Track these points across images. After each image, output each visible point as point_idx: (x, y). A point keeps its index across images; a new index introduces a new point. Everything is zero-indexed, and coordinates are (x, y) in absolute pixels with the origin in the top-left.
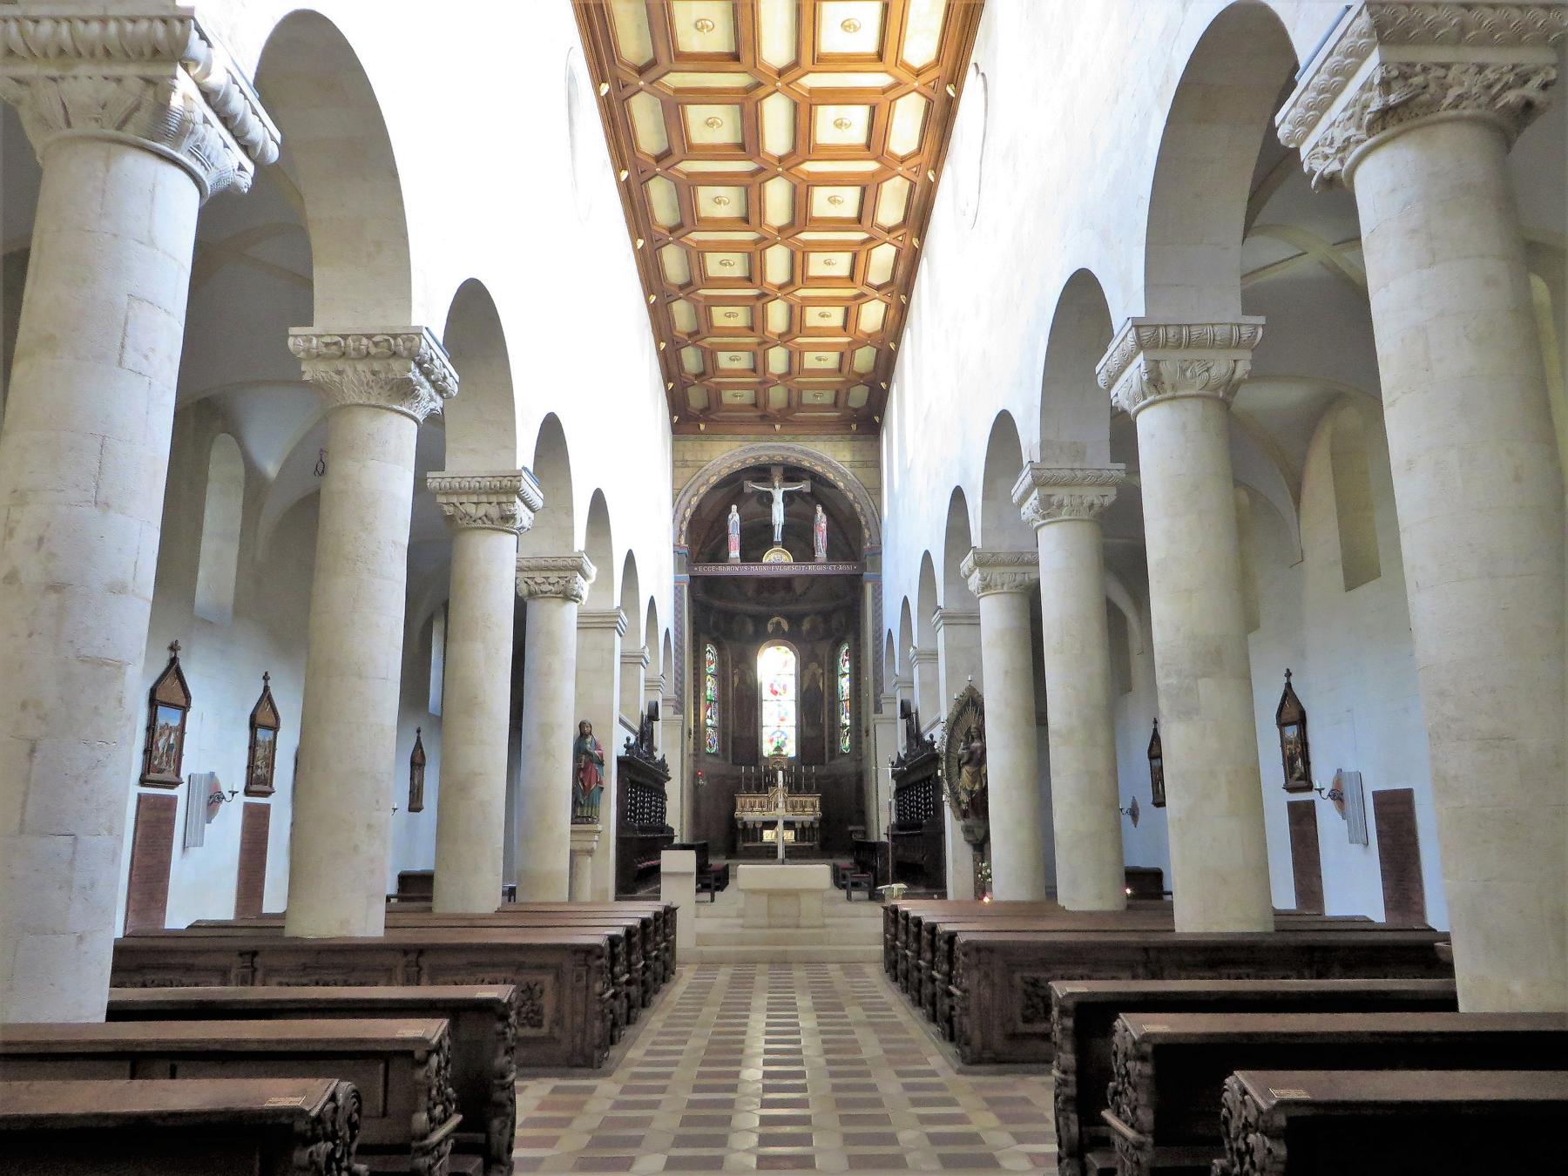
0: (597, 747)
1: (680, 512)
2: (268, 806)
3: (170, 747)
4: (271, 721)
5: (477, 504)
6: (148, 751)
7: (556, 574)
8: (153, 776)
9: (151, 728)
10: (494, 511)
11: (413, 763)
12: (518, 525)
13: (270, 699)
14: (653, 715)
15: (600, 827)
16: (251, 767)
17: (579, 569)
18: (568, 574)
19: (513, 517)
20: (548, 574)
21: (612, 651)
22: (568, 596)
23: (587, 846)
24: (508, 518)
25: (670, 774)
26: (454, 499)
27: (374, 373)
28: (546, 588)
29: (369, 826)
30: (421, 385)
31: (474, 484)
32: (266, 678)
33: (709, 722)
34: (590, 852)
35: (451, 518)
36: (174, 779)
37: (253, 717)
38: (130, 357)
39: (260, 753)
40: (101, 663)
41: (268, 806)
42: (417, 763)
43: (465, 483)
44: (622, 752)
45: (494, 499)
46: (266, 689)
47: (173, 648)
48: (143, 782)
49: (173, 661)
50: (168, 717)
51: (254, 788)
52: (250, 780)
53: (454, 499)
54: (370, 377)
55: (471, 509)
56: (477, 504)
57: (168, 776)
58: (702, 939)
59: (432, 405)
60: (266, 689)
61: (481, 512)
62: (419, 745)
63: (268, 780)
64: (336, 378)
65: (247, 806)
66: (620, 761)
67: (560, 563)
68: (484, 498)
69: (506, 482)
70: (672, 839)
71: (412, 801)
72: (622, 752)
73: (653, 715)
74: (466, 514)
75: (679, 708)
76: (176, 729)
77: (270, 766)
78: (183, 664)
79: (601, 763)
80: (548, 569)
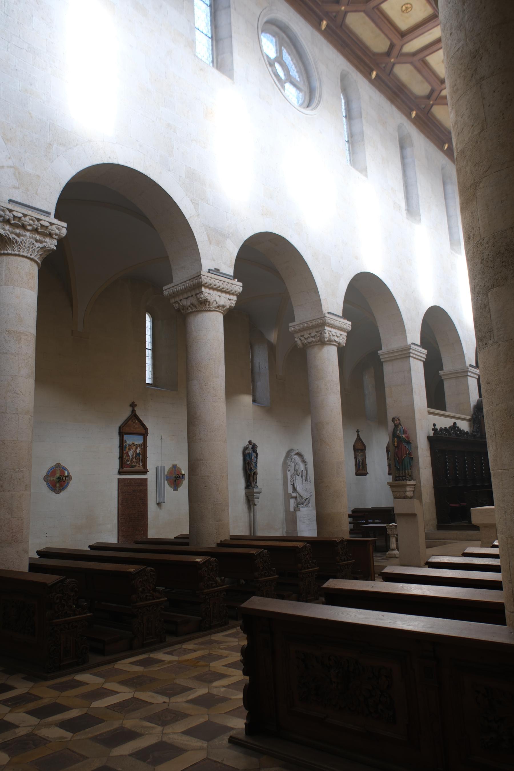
0: (405, 432)
3: (138, 455)
5: (187, 298)
6: (121, 458)
7: (315, 330)
8: (125, 469)
9: (122, 446)
10: (193, 300)
11: (355, 449)
12: (215, 305)
15: (412, 482)
18: (320, 329)
20: (311, 331)
22: (323, 342)
24: (205, 302)
28: (310, 340)
30: (18, 235)
35: (178, 310)
36: (144, 470)
45: (193, 293)
47: (133, 405)
48: (120, 473)
49: (133, 411)
50: (129, 440)
53: (177, 299)
57: (139, 467)
61: (189, 304)
62: (359, 439)
66: (429, 438)
67: (314, 323)
72: (431, 433)
74: (183, 306)
76: (140, 445)
78: (138, 413)
79: (408, 443)
80: (309, 328)
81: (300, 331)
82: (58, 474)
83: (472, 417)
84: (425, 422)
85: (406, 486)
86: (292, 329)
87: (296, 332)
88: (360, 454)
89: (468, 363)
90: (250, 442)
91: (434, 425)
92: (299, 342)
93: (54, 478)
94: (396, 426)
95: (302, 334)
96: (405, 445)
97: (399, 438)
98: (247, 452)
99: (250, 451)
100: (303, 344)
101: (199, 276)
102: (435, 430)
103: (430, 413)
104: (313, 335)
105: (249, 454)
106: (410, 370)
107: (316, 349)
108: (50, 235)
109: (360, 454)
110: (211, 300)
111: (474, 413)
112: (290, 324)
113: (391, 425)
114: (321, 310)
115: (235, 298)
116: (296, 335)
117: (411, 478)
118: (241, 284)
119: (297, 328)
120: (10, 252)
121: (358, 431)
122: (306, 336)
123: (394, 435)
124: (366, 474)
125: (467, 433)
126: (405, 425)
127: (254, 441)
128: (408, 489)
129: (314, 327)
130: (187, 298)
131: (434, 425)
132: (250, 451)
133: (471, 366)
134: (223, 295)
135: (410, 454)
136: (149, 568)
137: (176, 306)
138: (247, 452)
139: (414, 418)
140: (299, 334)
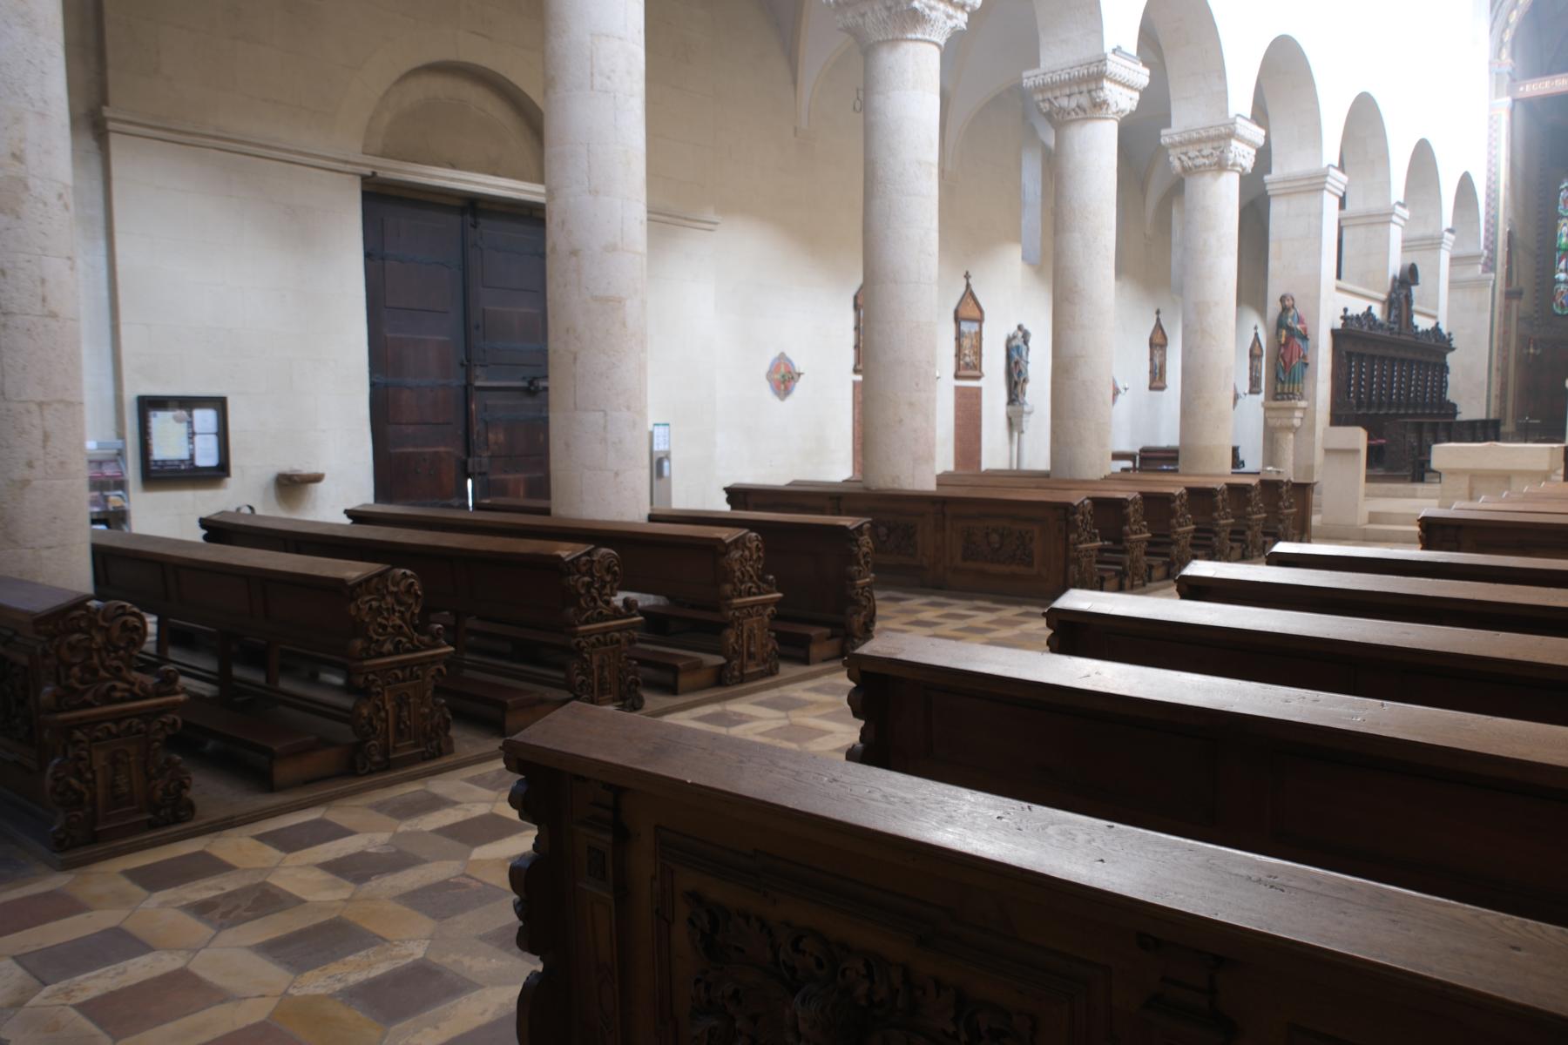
0: (1300, 320)
1: (1501, 19)
2: (979, 389)
4: (976, 314)
7: (1210, 145)
10: (1084, 100)
11: (1152, 345)
13: (972, 294)
14: (1409, 277)
15: (1302, 404)
16: (959, 354)
17: (1232, 135)
18: (1222, 143)
19: (1105, 102)
20: (1203, 146)
21: (1320, 215)
22: (1221, 166)
23: (1286, 422)
25: (1454, 344)
26: (1049, 95)
27: (889, 9)
28: (1200, 161)
29: (911, 404)
31: (1065, 76)
32: (967, 276)
33: (1562, 276)
34: (1291, 428)
37: (956, 312)
38: (598, 80)
39: (966, 343)
40: (607, 300)
41: (979, 389)
42: (1158, 343)
43: (1056, 78)
44: (1339, 324)
45: (1084, 88)
46: (968, 285)
51: (962, 373)
52: (958, 367)
53: (1049, 95)
54: (885, 14)
55: (1064, 102)
56: (1069, 96)
58: (1374, 518)
59: (951, 24)
60: (968, 285)
61: (1073, 104)
62: (1159, 327)
63: (977, 366)
64: (860, 21)
65: (957, 388)
66: (1334, 333)
67: (1212, 132)
68: (1075, 89)
69: (1093, 69)
70: (1455, 414)
71: (1153, 379)
73: (1409, 277)
75: (1490, 266)
77: (978, 352)
79: (1305, 338)
80: (1200, 141)
81: (1181, 144)
82: (783, 370)
83: (1390, 295)
84: (1331, 306)
85: (1293, 409)
86: (1165, 140)
87: (1173, 145)
88: (1157, 353)
89: (1393, 202)
90: (1020, 327)
91: (1345, 310)
92: (1176, 164)
93: (778, 377)
94: (1285, 310)
95: (1184, 149)
96: (1298, 341)
97: (1290, 329)
98: (1014, 343)
99: (1019, 342)
100: (1183, 168)
101: (1103, 60)
102: (1344, 318)
103: (1339, 289)
104: (1205, 152)
105: (1018, 347)
106: (1321, 214)
107: (1208, 178)
108: (962, 7)
109: (1157, 353)
110: (1111, 101)
111: (1393, 290)
112: (1164, 132)
113: (1274, 308)
114: (1226, 111)
115: (1136, 96)
116: (1171, 151)
117: (1302, 397)
118: (1147, 71)
119: (1177, 138)
120: (919, 36)
121: (1158, 312)
122: (1192, 154)
123: (1281, 324)
124: (1162, 388)
125: (1381, 325)
126: (1300, 308)
127: (1026, 327)
128: (1298, 414)
129: (1210, 139)
130: (1069, 96)
131: (1345, 310)
132: (1019, 342)
133: (1399, 203)
134: (1126, 91)
135: (1304, 357)
136: (604, 550)
137: (1045, 107)
138: (1014, 343)
139: (1318, 297)
140: (1178, 150)
